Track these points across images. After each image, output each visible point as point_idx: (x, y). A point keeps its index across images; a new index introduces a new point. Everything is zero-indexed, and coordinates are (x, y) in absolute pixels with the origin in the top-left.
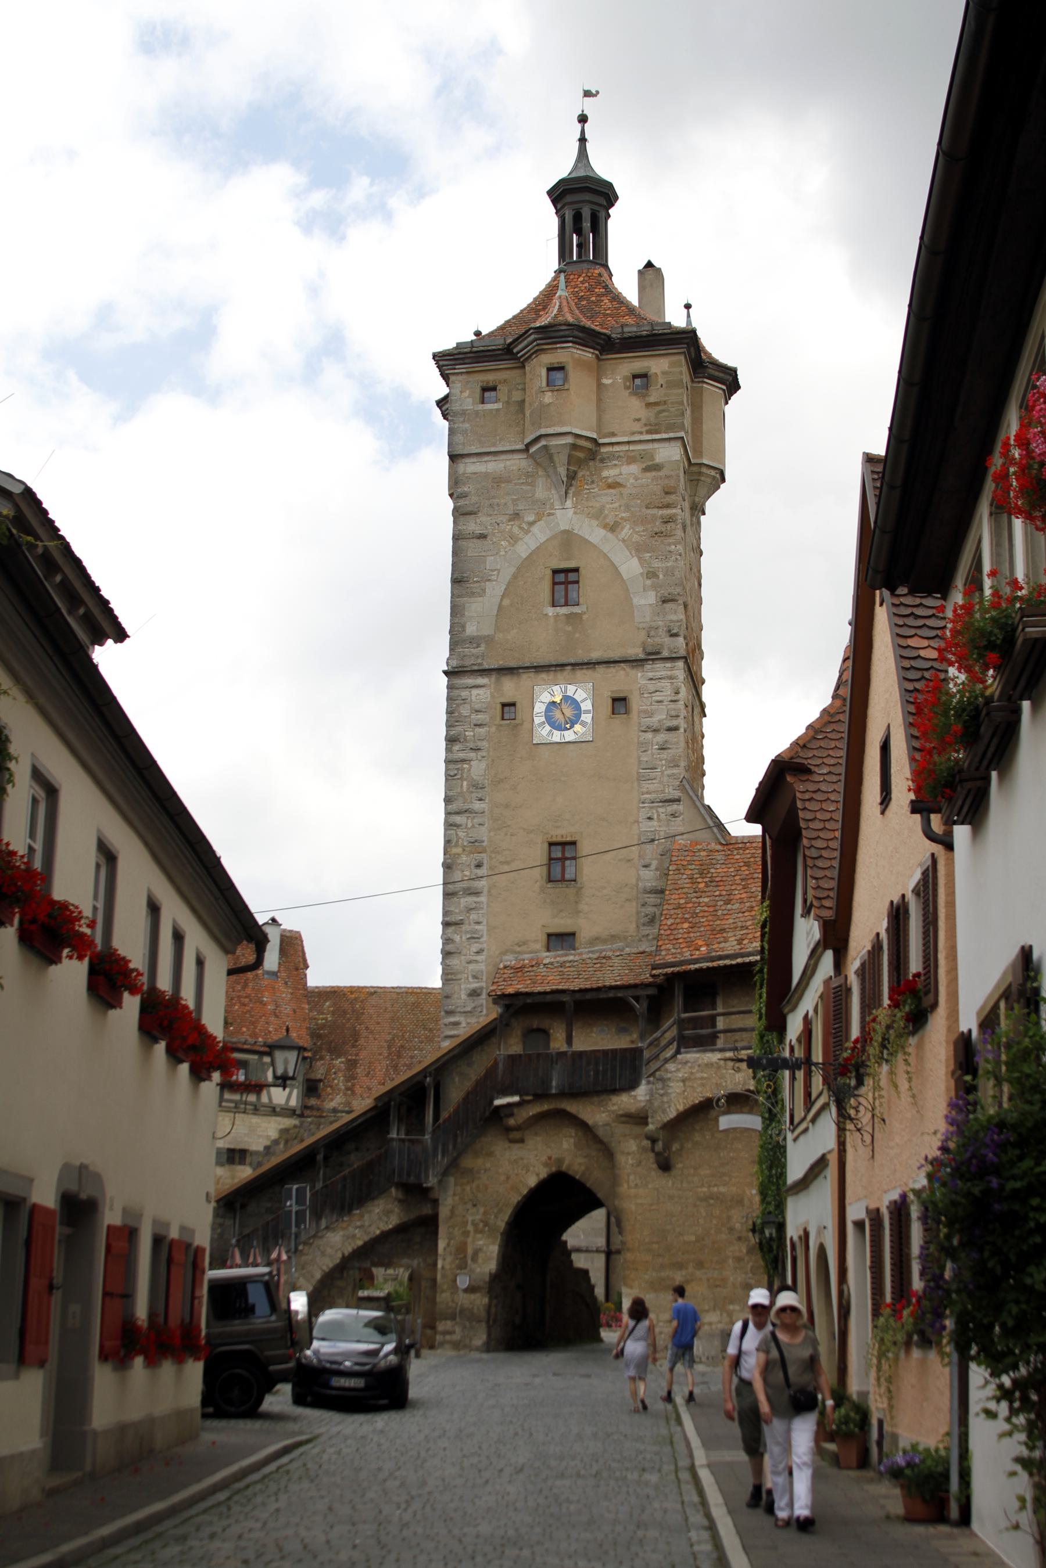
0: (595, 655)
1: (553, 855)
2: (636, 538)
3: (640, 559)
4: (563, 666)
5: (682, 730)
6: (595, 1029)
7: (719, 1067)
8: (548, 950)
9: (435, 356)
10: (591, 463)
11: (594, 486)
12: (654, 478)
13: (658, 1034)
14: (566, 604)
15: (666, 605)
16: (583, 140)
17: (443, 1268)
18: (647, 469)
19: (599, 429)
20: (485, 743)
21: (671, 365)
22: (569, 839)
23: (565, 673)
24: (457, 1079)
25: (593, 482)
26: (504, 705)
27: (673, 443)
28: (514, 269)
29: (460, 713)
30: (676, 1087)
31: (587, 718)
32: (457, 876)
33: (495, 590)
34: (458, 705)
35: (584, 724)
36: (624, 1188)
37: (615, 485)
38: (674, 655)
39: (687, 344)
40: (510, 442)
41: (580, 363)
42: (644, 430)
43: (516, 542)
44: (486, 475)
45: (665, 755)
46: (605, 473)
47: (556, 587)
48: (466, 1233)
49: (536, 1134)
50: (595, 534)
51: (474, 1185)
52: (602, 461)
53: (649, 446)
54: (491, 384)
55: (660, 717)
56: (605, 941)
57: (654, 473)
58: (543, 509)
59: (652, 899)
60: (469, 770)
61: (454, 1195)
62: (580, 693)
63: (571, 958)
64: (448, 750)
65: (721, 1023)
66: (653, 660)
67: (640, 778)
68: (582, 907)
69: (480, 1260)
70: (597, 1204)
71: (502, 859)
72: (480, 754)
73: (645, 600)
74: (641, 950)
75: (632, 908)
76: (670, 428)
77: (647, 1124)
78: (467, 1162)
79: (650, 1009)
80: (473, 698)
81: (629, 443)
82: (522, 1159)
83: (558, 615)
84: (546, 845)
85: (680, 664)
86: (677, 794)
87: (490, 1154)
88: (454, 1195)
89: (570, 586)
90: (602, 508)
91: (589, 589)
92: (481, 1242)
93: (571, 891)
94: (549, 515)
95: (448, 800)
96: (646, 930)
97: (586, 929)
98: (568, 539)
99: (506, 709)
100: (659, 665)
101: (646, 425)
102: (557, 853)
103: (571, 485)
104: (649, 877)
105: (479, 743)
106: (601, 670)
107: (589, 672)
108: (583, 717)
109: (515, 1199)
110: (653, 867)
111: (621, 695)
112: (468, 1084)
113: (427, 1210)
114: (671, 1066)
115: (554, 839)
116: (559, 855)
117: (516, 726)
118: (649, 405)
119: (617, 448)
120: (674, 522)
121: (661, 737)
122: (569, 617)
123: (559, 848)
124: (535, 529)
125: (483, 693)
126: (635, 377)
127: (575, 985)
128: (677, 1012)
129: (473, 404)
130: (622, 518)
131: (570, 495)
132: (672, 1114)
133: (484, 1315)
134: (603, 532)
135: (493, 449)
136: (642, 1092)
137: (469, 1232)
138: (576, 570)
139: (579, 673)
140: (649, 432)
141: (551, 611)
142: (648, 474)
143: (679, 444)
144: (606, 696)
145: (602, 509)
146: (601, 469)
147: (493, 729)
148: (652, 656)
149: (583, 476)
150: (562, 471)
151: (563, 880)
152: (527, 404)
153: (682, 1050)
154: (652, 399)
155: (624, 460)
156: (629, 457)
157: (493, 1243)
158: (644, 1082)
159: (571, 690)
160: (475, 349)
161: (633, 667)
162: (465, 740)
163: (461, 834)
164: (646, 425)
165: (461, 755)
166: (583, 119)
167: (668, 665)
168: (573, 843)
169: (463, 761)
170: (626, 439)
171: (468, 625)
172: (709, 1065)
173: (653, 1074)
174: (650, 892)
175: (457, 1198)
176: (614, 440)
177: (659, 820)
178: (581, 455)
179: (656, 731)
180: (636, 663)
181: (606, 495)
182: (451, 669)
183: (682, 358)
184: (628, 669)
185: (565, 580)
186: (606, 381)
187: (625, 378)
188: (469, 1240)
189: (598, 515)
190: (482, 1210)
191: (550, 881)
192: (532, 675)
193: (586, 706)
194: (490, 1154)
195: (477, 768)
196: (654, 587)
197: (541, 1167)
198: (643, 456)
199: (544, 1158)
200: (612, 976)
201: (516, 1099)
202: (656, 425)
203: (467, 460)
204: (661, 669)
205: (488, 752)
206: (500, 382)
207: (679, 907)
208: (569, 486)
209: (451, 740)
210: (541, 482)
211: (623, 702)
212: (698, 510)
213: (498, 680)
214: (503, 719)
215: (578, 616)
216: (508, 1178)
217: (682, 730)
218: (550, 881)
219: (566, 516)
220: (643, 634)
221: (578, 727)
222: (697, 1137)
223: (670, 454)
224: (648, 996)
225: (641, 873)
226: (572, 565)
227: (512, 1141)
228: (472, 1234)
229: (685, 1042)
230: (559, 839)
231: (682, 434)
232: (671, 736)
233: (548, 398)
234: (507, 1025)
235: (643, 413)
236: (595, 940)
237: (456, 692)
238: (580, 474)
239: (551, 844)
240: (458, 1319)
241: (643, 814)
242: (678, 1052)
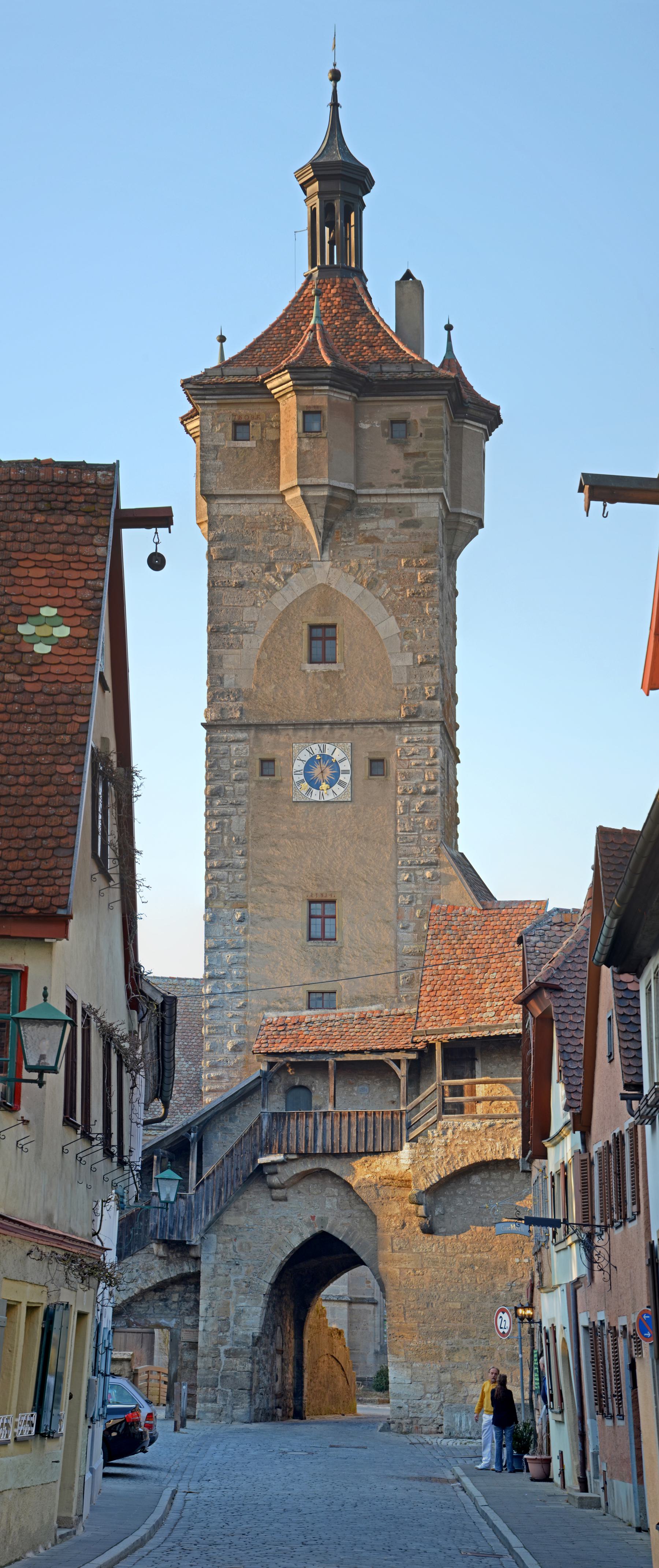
1: (313, 913)
2: (393, 597)
3: (398, 620)
4: (321, 724)
5: (439, 794)
6: (356, 1088)
8: (309, 1008)
9: (185, 383)
10: (348, 515)
11: (350, 539)
12: (412, 535)
13: (420, 1099)
14: (324, 661)
15: (422, 668)
17: (204, 1330)
18: (406, 525)
20: (244, 799)
21: (432, 411)
22: (329, 898)
23: (324, 732)
24: (219, 1134)
25: (350, 535)
26: (263, 761)
27: (432, 499)
28: (261, 277)
29: (219, 767)
30: (437, 1152)
31: (345, 778)
32: (218, 929)
33: (253, 643)
34: (217, 759)
35: (342, 784)
36: (386, 1253)
37: (372, 539)
38: (431, 719)
39: (449, 391)
40: (265, 485)
42: (402, 482)
43: (272, 594)
44: (241, 519)
46: (362, 526)
47: (314, 642)
48: (229, 1294)
49: (299, 1192)
50: (352, 590)
51: (237, 1244)
52: (359, 512)
53: (408, 500)
54: (243, 419)
57: (412, 530)
58: (301, 561)
60: (230, 824)
61: (216, 1253)
63: (332, 1017)
64: (209, 805)
66: (410, 723)
68: (341, 966)
69: (242, 1323)
70: (356, 1261)
71: (264, 915)
72: (241, 810)
74: (400, 1011)
76: (429, 483)
78: (229, 1219)
79: (410, 1072)
80: (233, 753)
81: (386, 495)
82: (285, 1217)
83: (315, 673)
84: (306, 905)
87: (253, 1212)
88: (216, 1253)
89: (327, 642)
92: (244, 1304)
93: (331, 949)
94: (307, 566)
95: (209, 856)
98: (326, 595)
99: (266, 764)
100: (416, 728)
101: (404, 477)
102: (317, 909)
103: (328, 536)
105: (239, 799)
106: (359, 729)
107: (347, 732)
108: (342, 777)
109: (280, 1259)
110: (411, 929)
111: (379, 757)
112: (231, 1141)
113: (187, 1268)
115: (314, 898)
116: (319, 913)
117: (275, 784)
118: (407, 455)
119: (374, 500)
120: (433, 582)
123: (319, 906)
125: (241, 747)
126: (393, 422)
128: (438, 1080)
129: (226, 439)
130: (379, 575)
131: (328, 547)
133: (246, 1384)
134: (360, 588)
135: (247, 492)
137: (231, 1292)
138: (334, 626)
139: (337, 733)
140: (407, 485)
141: (309, 668)
142: (406, 530)
143: (437, 499)
144: (364, 757)
147: (253, 785)
149: (340, 527)
151: (323, 938)
152: (282, 447)
153: (444, 1116)
154: (411, 450)
155: (382, 513)
156: (386, 510)
157: (257, 1306)
158: (406, 1145)
159: (329, 749)
160: (226, 380)
161: (389, 729)
162: (225, 795)
163: (222, 889)
164: (404, 477)
165: (222, 810)
167: (425, 728)
169: (224, 815)
170: (384, 491)
171: (226, 676)
174: (408, 954)
175: (219, 1256)
176: (371, 491)
177: (416, 882)
178: (338, 507)
181: (363, 549)
182: (211, 723)
183: (442, 404)
184: (385, 731)
185: (322, 638)
186: (365, 426)
187: (383, 424)
188: (231, 1301)
190: (245, 1269)
191: (310, 939)
192: (291, 732)
193: (345, 766)
194: (253, 1212)
195: (237, 824)
196: (411, 648)
197: (304, 1227)
199: (307, 1218)
201: (280, 1157)
202: (415, 478)
203: (221, 501)
204: (420, 732)
205: (248, 807)
206: (253, 418)
209: (212, 795)
211: (380, 763)
213: (256, 737)
214: (262, 775)
215: (337, 674)
216: (271, 1237)
217: (439, 794)
218: (310, 939)
221: (336, 787)
222: (459, 1202)
223: (429, 509)
224: (408, 1060)
225: (400, 934)
226: (328, 620)
227: (274, 1199)
228: (234, 1295)
230: (319, 898)
231: (441, 490)
232: (430, 798)
234: (270, 1082)
235: (402, 464)
237: (215, 746)
238: (337, 525)
239: (311, 902)
240: (219, 1387)
242: (439, 1118)
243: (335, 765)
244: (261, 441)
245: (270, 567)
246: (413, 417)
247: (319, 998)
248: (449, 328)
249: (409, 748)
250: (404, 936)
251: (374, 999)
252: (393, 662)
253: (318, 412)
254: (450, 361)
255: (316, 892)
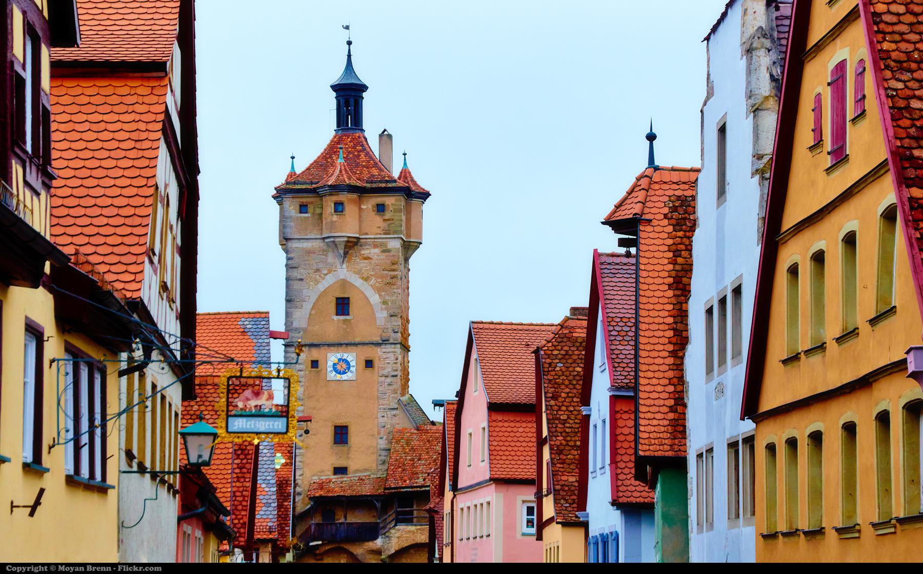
0: (358, 340)
2: (377, 284)
3: (380, 295)
7: (413, 532)
16: (349, 56)
18: (383, 251)
19: (360, 232)
41: (351, 201)
45: (390, 387)
46: (363, 252)
50: (357, 282)
55: (388, 370)
56: (361, 472)
59: (384, 453)
62: (351, 356)
65: (415, 512)
67: (378, 398)
73: (381, 315)
75: (374, 457)
76: (395, 232)
77: (381, 555)
85: (399, 346)
86: (396, 406)
90: (361, 270)
91: (354, 307)
96: (381, 467)
97: (352, 465)
98: (344, 283)
100: (388, 346)
104: (383, 444)
106: (360, 347)
114: (393, 531)
118: (384, 220)
121: (389, 380)
122: (344, 321)
124: (328, 277)
126: (378, 205)
127: (348, 493)
132: (393, 551)
134: (361, 281)
136: (379, 542)
138: (348, 298)
139: (350, 348)
140: (385, 234)
141: (336, 318)
144: (363, 359)
145: (361, 270)
146: (360, 250)
148: (385, 342)
150: (342, 252)
166: (349, 43)
168: (347, 427)
172: (409, 532)
173: (384, 534)
179: (386, 376)
180: (378, 344)
185: (343, 306)
186: (363, 207)
187: (373, 206)
189: (359, 272)
196: (386, 309)
198: (381, 245)
200: (366, 490)
204: (389, 348)
207: (397, 460)
208: (345, 257)
210: (330, 254)
212: (406, 260)
219: (344, 272)
220: (381, 331)
221: (349, 374)
229: (398, 521)
233: (335, 218)
236: (357, 471)
241: (380, 415)
243: (348, 363)
244: (313, 214)
245: (318, 270)
246: (387, 203)
247: (340, 471)
248: (405, 154)
249: (386, 357)
250: (381, 441)
251: (366, 470)
252: (377, 315)
253: (342, 204)
254: (405, 174)
255: (340, 422)
